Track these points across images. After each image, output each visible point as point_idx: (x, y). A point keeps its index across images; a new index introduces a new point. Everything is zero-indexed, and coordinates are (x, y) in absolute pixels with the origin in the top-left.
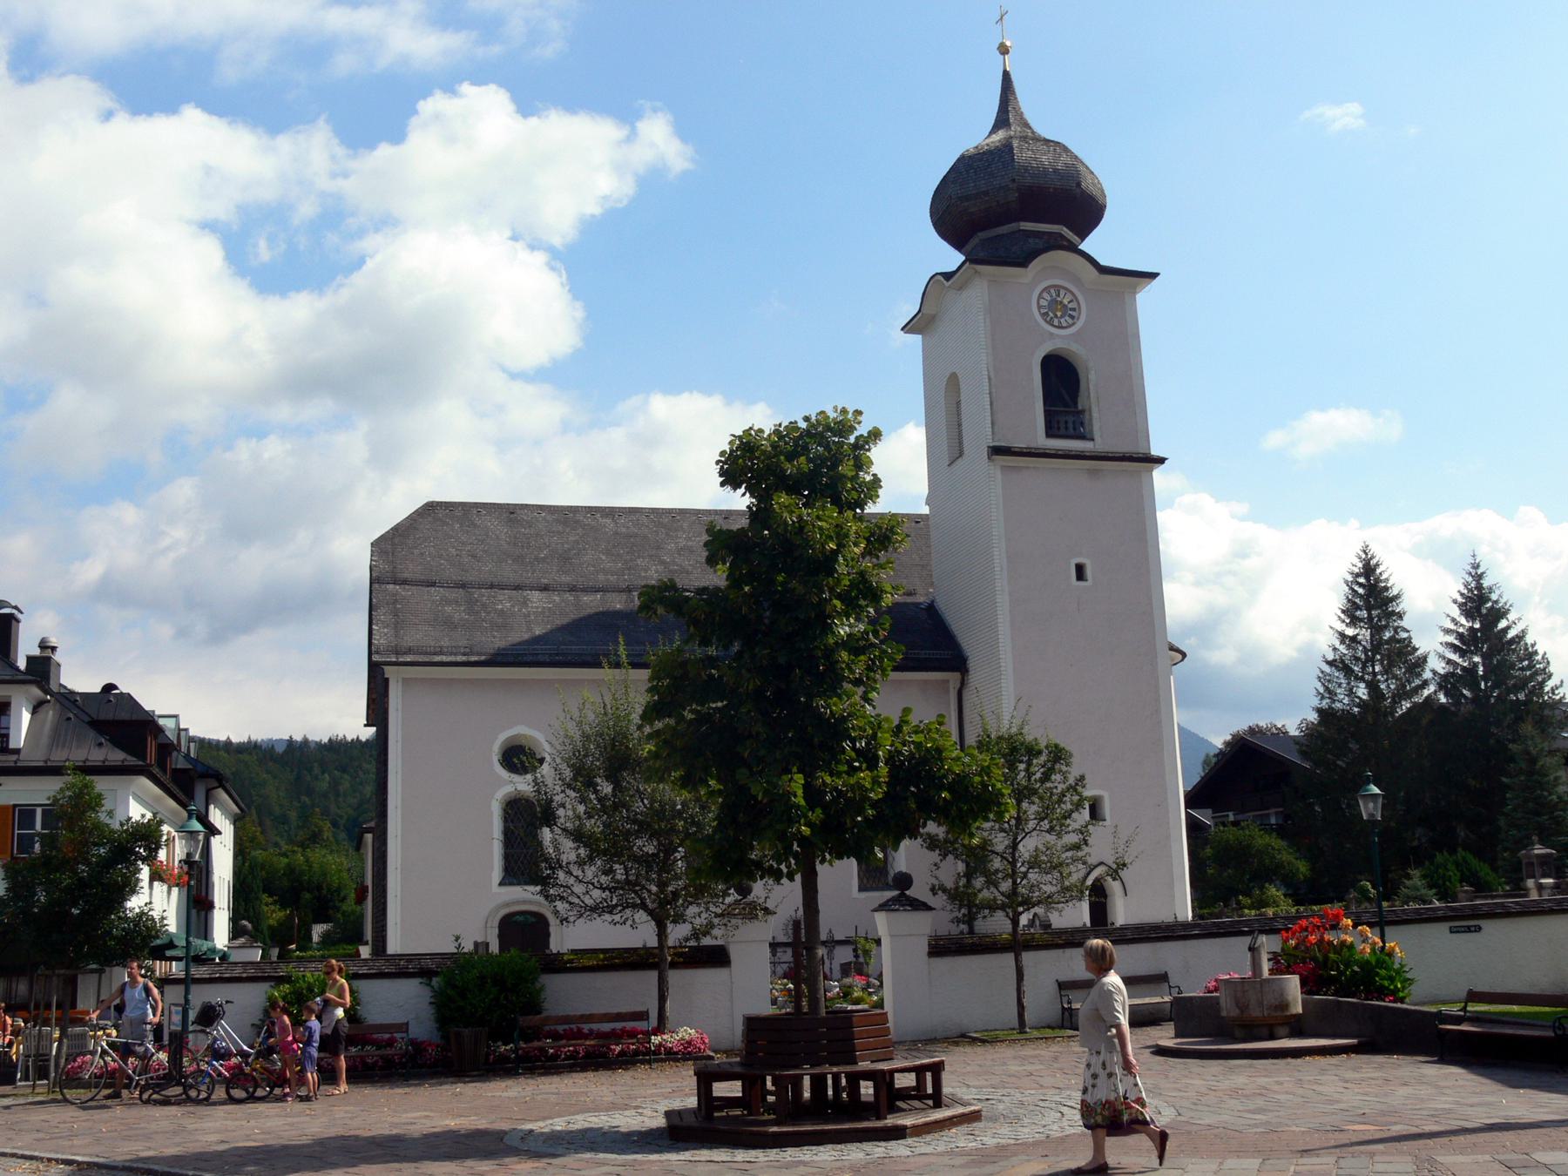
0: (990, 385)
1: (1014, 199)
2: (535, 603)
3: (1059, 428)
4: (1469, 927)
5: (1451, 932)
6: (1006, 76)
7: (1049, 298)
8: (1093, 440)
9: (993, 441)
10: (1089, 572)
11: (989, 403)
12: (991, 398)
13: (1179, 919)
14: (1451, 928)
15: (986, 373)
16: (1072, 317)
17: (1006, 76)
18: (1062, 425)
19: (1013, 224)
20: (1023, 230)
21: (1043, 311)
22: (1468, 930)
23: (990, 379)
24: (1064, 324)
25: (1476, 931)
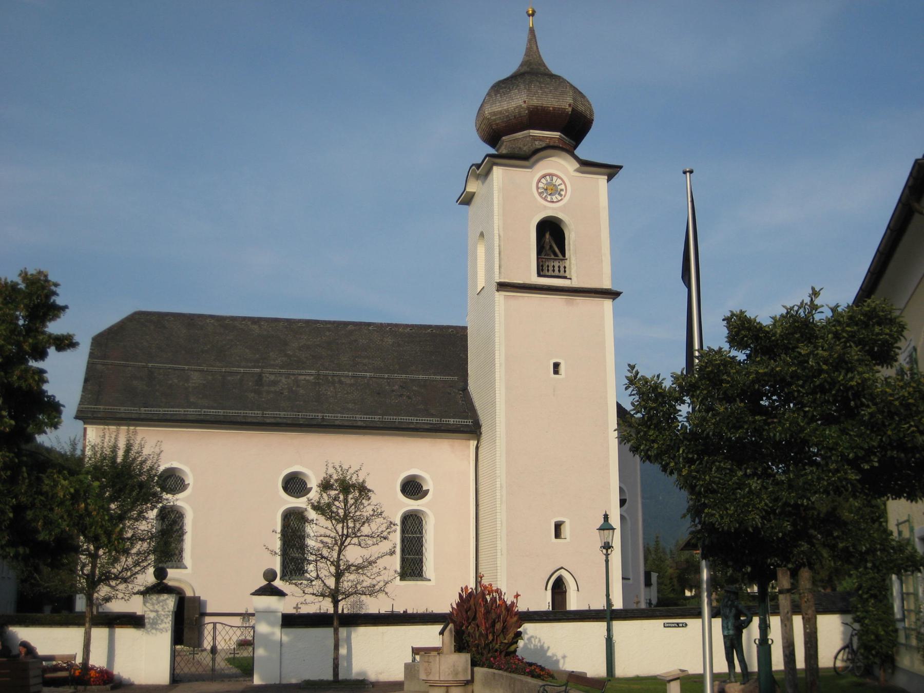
0: (499, 240)
1: (525, 114)
2: (195, 380)
3: (548, 270)
4: (678, 624)
5: (665, 627)
6: (532, 31)
7: (549, 180)
8: (570, 279)
9: (499, 278)
10: (562, 369)
11: (498, 252)
12: (499, 249)
13: (381, 612)
14: (664, 624)
15: (497, 232)
16: (561, 195)
17: (532, 31)
18: (551, 268)
19: (525, 132)
20: (531, 135)
21: (540, 191)
22: (678, 625)
23: (499, 236)
24: (555, 200)
25: (683, 627)
